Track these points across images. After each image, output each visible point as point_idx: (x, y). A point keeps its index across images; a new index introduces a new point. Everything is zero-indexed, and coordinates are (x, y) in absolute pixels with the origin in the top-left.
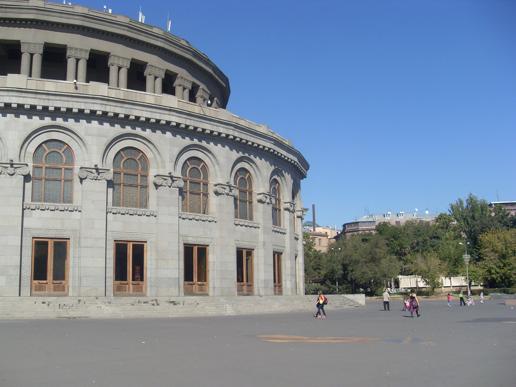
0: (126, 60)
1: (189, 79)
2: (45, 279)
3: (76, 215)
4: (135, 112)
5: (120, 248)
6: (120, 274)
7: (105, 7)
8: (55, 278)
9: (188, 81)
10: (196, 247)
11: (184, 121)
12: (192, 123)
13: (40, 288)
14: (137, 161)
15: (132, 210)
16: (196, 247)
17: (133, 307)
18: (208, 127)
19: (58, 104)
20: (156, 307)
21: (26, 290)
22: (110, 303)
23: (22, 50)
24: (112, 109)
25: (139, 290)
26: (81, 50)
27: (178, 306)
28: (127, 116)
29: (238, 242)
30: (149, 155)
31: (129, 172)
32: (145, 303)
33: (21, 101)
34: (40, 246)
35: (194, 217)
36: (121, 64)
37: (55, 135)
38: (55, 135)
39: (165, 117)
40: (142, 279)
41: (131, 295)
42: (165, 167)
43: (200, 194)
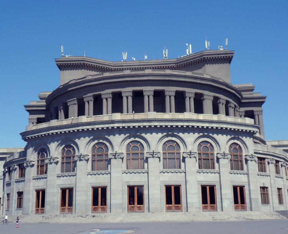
0: (130, 93)
1: (172, 90)
5: (95, 190)
6: (95, 202)
7: (187, 44)
10: (136, 187)
14: (103, 148)
15: (99, 172)
16: (136, 187)
17: (74, 218)
20: (84, 218)
22: (66, 216)
27: (94, 218)
29: (166, 182)
31: (99, 153)
32: (81, 216)
35: (133, 172)
36: (127, 94)
40: (105, 205)
41: (100, 213)
43: (139, 159)
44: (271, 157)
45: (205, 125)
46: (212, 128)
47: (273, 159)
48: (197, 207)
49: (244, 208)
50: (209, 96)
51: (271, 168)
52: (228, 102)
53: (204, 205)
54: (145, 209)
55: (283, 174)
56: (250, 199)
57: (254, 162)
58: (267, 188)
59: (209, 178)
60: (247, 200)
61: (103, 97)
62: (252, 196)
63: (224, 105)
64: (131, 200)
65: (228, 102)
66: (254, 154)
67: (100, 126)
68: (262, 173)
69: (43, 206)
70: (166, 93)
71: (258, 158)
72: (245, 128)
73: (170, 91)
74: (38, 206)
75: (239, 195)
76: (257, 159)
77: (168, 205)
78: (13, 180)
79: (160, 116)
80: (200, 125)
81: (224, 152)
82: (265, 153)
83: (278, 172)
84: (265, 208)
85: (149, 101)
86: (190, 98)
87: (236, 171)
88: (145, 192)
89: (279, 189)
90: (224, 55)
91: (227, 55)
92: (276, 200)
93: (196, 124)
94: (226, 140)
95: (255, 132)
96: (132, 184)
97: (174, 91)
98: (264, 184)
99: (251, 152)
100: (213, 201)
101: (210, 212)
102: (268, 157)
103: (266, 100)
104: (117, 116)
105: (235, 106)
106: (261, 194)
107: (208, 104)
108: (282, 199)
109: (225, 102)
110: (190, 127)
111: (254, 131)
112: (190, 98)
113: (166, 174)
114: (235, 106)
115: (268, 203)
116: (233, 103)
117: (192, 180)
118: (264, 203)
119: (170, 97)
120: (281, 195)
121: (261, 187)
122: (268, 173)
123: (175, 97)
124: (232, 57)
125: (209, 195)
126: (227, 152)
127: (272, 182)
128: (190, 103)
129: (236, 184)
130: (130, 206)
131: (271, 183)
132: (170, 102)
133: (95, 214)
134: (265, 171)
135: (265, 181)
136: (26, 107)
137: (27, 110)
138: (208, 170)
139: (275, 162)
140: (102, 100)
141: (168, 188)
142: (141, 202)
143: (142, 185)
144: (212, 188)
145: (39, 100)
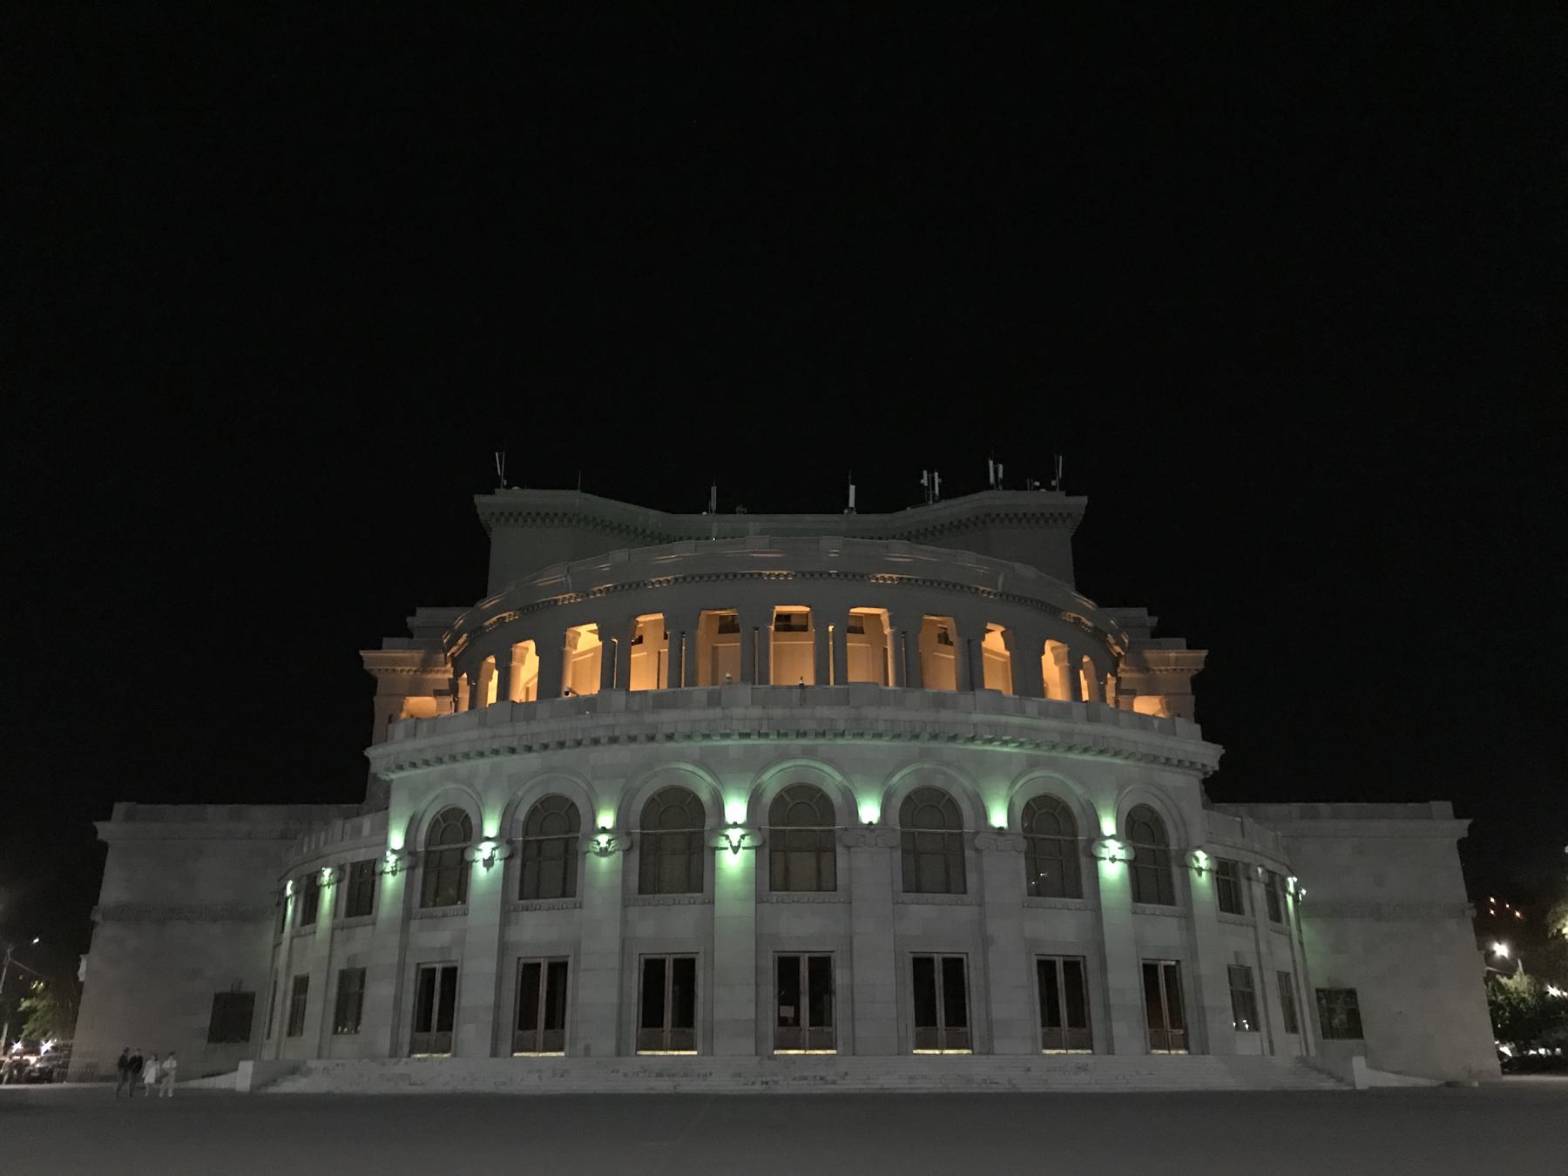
5: (653, 970)
8: (550, 1024)
21: (506, 1047)
56: (1202, 1010)
62: (1208, 1001)
69: (447, 1024)
74: (422, 1023)
84: (1249, 1045)
87: (1150, 907)
88: (840, 977)
89: (1284, 978)
92: (1277, 1017)
98: (1237, 954)
125: (1064, 994)
127: (1263, 949)
131: (1259, 953)
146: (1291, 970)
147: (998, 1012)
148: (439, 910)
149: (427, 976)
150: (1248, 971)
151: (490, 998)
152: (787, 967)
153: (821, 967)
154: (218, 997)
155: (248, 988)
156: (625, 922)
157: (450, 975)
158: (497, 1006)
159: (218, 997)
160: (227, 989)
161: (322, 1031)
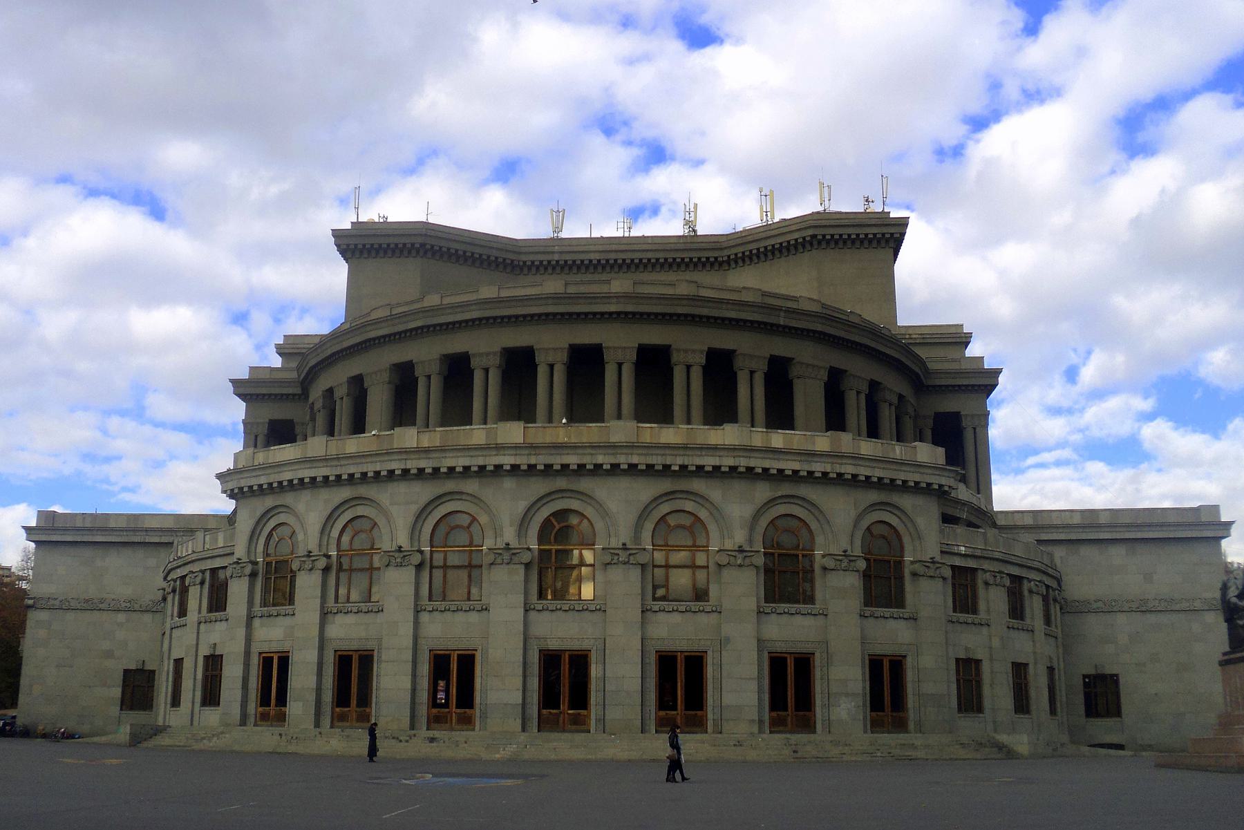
2: (349, 706)
3: (380, 618)
4: (446, 462)
9: (694, 351)
11: (523, 461)
12: (540, 460)
13: (343, 718)
18: (572, 460)
19: (352, 470)
21: (326, 721)
23: (417, 374)
24: (413, 465)
25: (467, 721)
26: (488, 354)
28: (436, 470)
30: (483, 519)
33: (312, 473)
34: (344, 661)
36: (550, 359)
37: (360, 511)
38: (360, 511)
39: (492, 461)
42: (502, 536)
44: (995, 567)
45: (789, 465)
46: (810, 473)
47: (1000, 572)
48: (753, 721)
49: (900, 725)
50: (814, 366)
51: (994, 601)
52: (874, 385)
53: (774, 714)
54: (593, 722)
55: (1032, 618)
57: (939, 584)
58: (978, 662)
59: (791, 629)
60: (911, 701)
61: (474, 363)
63: (863, 397)
64: (549, 698)
65: (874, 385)
66: (938, 558)
67: (460, 462)
68: (962, 617)
69: (282, 700)
70: (675, 357)
71: (953, 567)
72: (912, 477)
73: (689, 348)
74: (265, 700)
75: (886, 685)
76: (948, 573)
77: (662, 713)
78: (192, 617)
79: (652, 433)
80: (774, 465)
81: (845, 551)
82: (978, 553)
83: (1017, 611)
85: (619, 382)
86: (752, 373)
88: (595, 671)
89: (1019, 670)
90: (875, 230)
91: (885, 230)
93: (758, 463)
94: (853, 514)
95: (946, 488)
96: (553, 645)
97: (702, 352)
99: (931, 549)
100: (805, 701)
101: (788, 736)
102: (986, 565)
103: (1001, 379)
104: (513, 432)
105: (901, 397)
106: (958, 680)
107: (808, 396)
108: (1027, 698)
109: (865, 388)
110: (742, 469)
111: (941, 486)
112: (752, 373)
113: (661, 616)
114: (901, 397)
115: (980, 709)
116: (894, 385)
117: (737, 637)
118: (966, 711)
119: (688, 367)
120: (1026, 685)
121: (957, 660)
122: (983, 615)
123: (707, 370)
124: (903, 234)
126: (858, 551)
128: (750, 392)
129: (878, 650)
130: (544, 712)
132: (688, 385)
133: (436, 734)
134: (975, 611)
135: (973, 642)
136: (235, 382)
137: (239, 396)
138: (793, 607)
139: (1007, 582)
140: (471, 373)
141: (666, 662)
142: (580, 698)
143: (584, 647)
144: (804, 663)
145: (277, 362)
146: (1031, 661)
147: (729, 699)
148: (274, 610)
149: (267, 662)
150: (978, 662)
151: (313, 680)
152: (550, 660)
153: (580, 661)
154: (126, 672)
155: (148, 667)
156: (416, 623)
157: (284, 661)
158: (319, 690)
159: (126, 672)
160: (133, 667)
161: (193, 703)
